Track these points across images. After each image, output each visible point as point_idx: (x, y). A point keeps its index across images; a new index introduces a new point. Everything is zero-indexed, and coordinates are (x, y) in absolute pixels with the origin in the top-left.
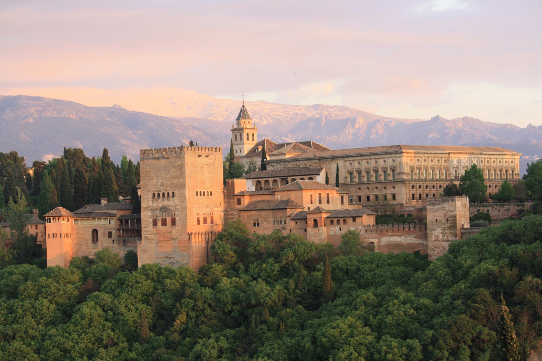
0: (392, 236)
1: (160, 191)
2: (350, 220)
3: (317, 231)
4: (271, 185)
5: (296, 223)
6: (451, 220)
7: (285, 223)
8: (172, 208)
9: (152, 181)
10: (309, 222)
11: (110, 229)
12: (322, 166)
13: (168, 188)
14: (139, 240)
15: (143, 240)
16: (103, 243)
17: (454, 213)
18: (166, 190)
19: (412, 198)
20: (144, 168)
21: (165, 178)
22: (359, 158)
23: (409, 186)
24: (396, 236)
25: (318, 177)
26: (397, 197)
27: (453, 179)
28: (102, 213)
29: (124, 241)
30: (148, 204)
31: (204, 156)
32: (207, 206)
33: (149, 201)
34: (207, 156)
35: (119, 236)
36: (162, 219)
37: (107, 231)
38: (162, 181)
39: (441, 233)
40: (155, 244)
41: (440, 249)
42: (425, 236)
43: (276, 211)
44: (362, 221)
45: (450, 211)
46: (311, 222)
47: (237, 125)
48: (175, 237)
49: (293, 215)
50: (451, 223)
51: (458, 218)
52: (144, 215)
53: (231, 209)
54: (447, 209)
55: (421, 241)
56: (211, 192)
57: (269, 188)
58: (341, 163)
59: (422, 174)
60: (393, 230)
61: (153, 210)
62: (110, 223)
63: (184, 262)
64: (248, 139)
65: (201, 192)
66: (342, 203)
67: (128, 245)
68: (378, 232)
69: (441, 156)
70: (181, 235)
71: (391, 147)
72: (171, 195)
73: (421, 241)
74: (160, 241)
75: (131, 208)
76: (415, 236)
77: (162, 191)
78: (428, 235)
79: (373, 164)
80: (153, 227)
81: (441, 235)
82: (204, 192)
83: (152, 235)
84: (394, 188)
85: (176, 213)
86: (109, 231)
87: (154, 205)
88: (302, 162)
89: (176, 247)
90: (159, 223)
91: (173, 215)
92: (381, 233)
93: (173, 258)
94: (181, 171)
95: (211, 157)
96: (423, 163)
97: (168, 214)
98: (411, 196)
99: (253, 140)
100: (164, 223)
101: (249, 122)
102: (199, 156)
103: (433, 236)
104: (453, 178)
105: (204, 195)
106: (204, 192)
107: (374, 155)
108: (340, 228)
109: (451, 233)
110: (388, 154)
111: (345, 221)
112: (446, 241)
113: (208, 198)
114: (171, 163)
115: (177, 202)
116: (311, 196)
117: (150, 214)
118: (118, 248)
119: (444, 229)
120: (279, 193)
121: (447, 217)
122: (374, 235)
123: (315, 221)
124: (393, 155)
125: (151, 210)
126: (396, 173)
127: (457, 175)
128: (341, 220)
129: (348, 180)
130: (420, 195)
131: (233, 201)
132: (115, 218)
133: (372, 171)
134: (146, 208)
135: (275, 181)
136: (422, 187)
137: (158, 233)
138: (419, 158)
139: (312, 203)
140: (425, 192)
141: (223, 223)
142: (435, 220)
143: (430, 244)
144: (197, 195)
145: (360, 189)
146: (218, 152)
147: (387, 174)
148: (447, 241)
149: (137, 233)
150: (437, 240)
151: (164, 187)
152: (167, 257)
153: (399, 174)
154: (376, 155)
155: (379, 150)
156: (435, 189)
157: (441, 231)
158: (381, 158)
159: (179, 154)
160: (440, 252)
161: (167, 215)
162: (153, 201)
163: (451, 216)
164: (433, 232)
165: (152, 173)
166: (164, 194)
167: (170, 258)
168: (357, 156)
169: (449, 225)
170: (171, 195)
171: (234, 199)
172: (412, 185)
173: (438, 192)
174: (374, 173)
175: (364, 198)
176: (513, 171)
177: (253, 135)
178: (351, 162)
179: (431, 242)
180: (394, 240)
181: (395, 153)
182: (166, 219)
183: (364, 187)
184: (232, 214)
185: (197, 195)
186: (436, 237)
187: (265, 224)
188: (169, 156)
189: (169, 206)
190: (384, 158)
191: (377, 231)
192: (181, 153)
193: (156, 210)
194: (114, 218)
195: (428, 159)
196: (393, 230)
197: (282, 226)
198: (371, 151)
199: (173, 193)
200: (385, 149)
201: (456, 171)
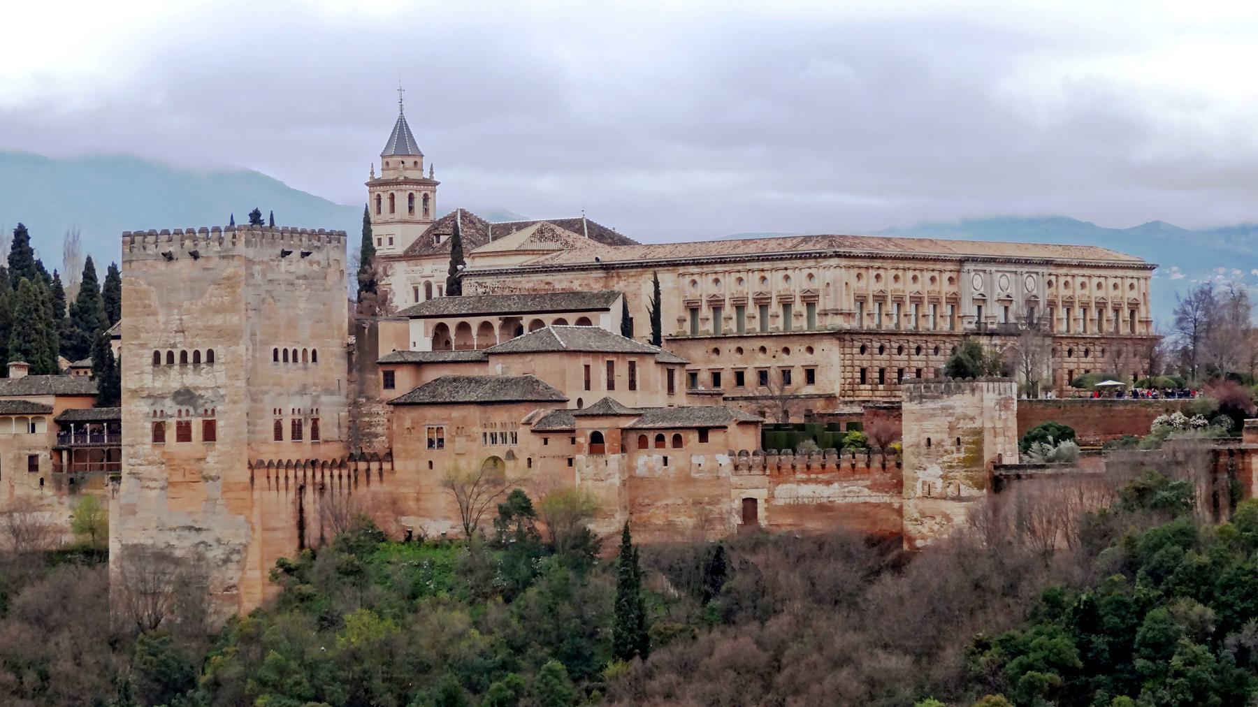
0: (806, 482)
1: (174, 346)
2: (693, 437)
3: (602, 466)
4: (475, 337)
5: (546, 443)
6: (970, 443)
7: (515, 440)
8: (208, 394)
9: (152, 319)
10: (580, 440)
11: (35, 448)
12: (616, 289)
13: (197, 339)
14: (113, 479)
15: (123, 479)
16: (12, 486)
17: (977, 424)
18: (192, 345)
19: (859, 380)
20: (132, 283)
21: (188, 312)
22: (719, 268)
23: (852, 347)
24: (817, 481)
25: (603, 316)
26: (818, 377)
27: (973, 330)
28: (13, 402)
29: (72, 481)
30: (141, 380)
31: (296, 254)
32: (303, 391)
33: (142, 373)
34: (305, 255)
35: (58, 468)
36: (179, 423)
37: (25, 454)
38: (181, 319)
39: (941, 477)
40: (157, 491)
41: (938, 519)
42: (898, 486)
43: (490, 409)
44: (726, 440)
45: (965, 417)
46: (583, 440)
47: (383, 170)
48: (213, 474)
49: (534, 422)
50: (967, 450)
51: (988, 437)
52: (130, 413)
53: (368, 399)
54: (959, 411)
55: (886, 499)
56: (314, 353)
57: (469, 343)
58: (667, 279)
59: (887, 315)
60: (808, 467)
61: (153, 397)
62: (33, 431)
63: (237, 542)
64: (411, 209)
65: (285, 351)
66: (671, 389)
67: (84, 491)
68: (768, 472)
69: (939, 266)
70: (230, 468)
71: (807, 239)
72: (204, 358)
73: (886, 499)
74: (171, 484)
75: (95, 392)
76: (868, 483)
77: (181, 348)
78: (906, 482)
79: (752, 285)
80: (154, 446)
81: (939, 483)
82: (295, 352)
83: (150, 468)
84: (810, 350)
85: (219, 408)
86: (30, 453)
87: (158, 384)
88: (559, 276)
89: (216, 499)
90: (171, 434)
91: (209, 412)
92: (776, 472)
93: (208, 530)
94: (234, 292)
95: (315, 256)
96: (1079, 292)
97: (195, 409)
98: (859, 375)
99: (426, 211)
100: (184, 433)
101: (415, 163)
102: (285, 254)
103: (919, 484)
104: (973, 326)
105: (295, 360)
106: (295, 352)
107: (758, 260)
108: (665, 459)
109: (967, 477)
110: (796, 258)
111: (678, 441)
112: (953, 499)
113: (305, 368)
114: (205, 269)
115: (222, 379)
116: (587, 367)
117: (144, 407)
118: (55, 499)
119: (950, 467)
120: (500, 359)
121: (956, 435)
122: (758, 478)
123: (597, 438)
124: (811, 263)
125: (149, 396)
126: (817, 311)
127: (983, 320)
128: (669, 438)
129: (687, 327)
130: (882, 371)
131: (373, 376)
132: (49, 419)
133: (751, 303)
134: (134, 393)
135: (486, 327)
136: (1091, 355)
137: (168, 461)
138: (881, 272)
139: (588, 387)
140: (894, 363)
141: (344, 437)
142: (924, 442)
143: (911, 507)
144: (276, 359)
145: (717, 351)
146: (334, 243)
147: (793, 312)
148: (958, 499)
149: (109, 460)
150: (928, 496)
151: (185, 337)
152: (190, 528)
153: (825, 313)
154: (763, 260)
155: (772, 248)
156: (921, 357)
157: (941, 473)
158: (777, 270)
159: (230, 245)
160: (936, 527)
161: (192, 411)
162: (154, 374)
163: (966, 434)
164: (920, 473)
165: (154, 296)
166: (184, 354)
167: (199, 530)
168: (711, 263)
169: (962, 455)
170: (204, 358)
171: (377, 374)
172: (860, 344)
173: (931, 364)
174: (758, 310)
175: (727, 378)
176: (1132, 313)
177: (426, 198)
178: (696, 277)
179: (911, 502)
180: (811, 494)
181: (815, 257)
182: (188, 424)
183: (728, 347)
184: (370, 414)
185: (276, 359)
186: (926, 488)
187: (461, 443)
188: (202, 252)
189: (197, 388)
190: (786, 269)
191: (765, 468)
192: (234, 244)
193: (163, 397)
194: (46, 417)
195: (903, 275)
196: (808, 467)
197: (506, 447)
198: (752, 250)
199: (211, 354)
200: (789, 244)
201: (979, 307)
